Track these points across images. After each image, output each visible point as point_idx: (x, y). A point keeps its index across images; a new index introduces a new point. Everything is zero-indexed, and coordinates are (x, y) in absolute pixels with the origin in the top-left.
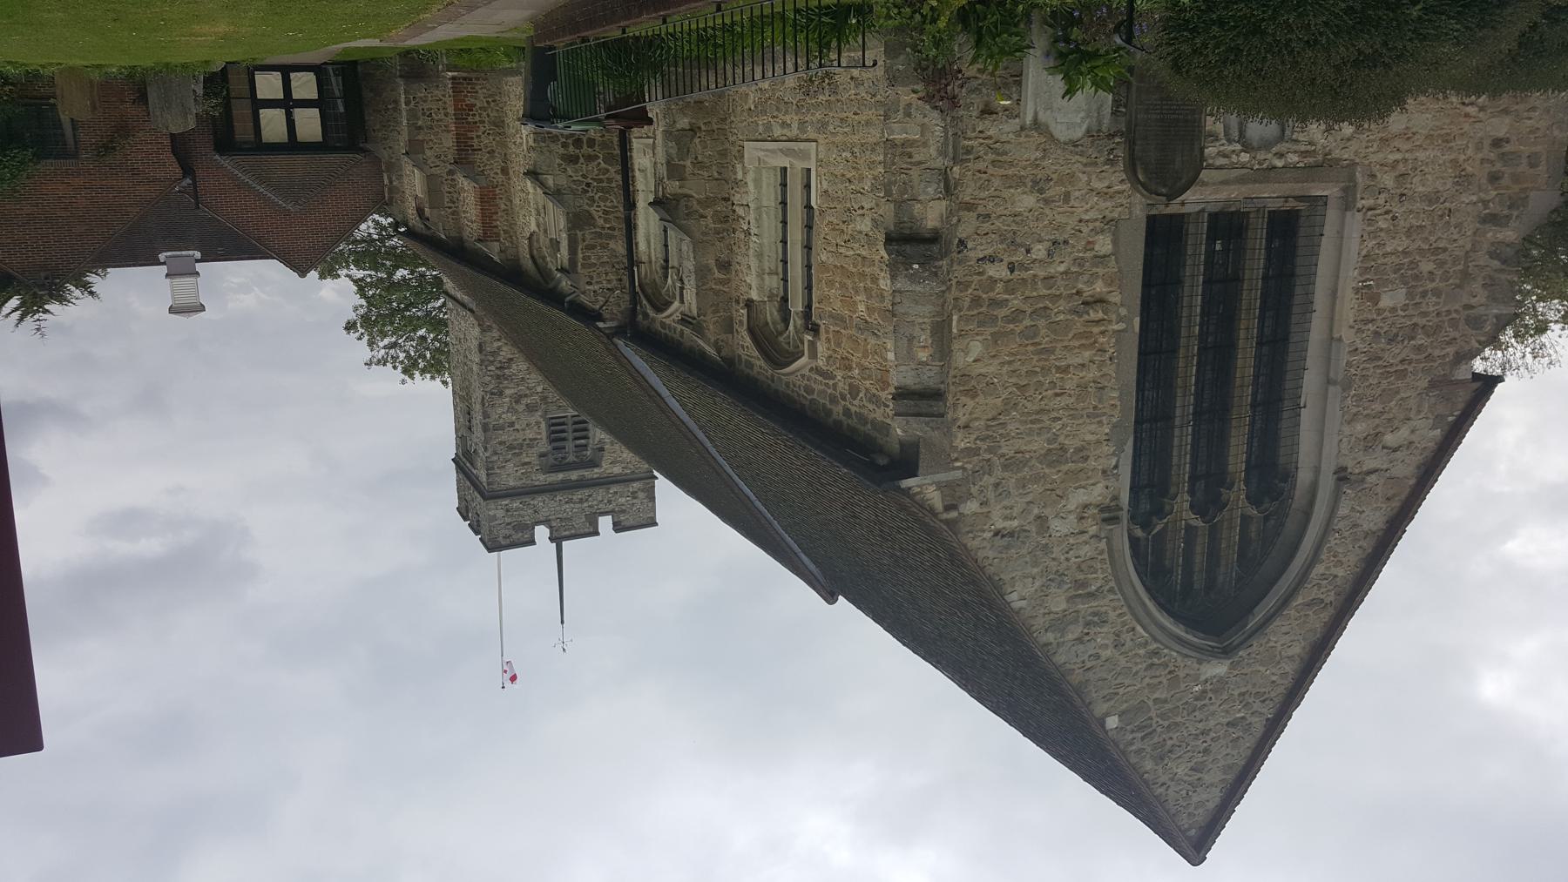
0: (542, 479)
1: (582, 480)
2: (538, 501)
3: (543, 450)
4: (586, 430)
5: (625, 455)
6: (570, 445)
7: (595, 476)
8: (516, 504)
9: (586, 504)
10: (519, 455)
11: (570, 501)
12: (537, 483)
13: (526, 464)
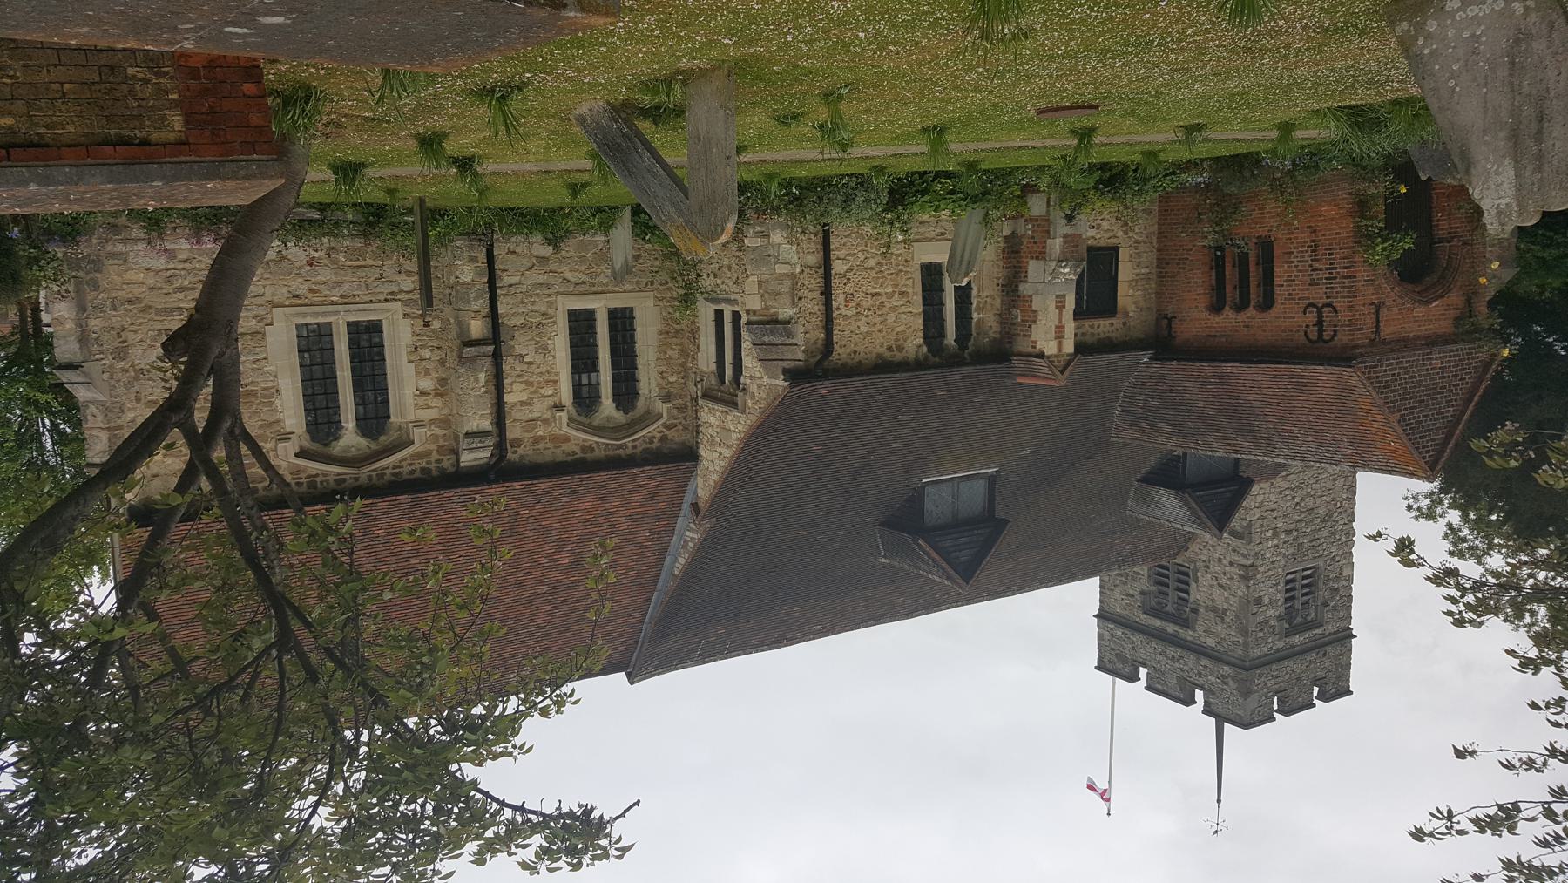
0: (1142, 618)
1: (1175, 636)
2: (1137, 638)
3: (1145, 588)
4: (1188, 584)
5: (1219, 628)
6: (1173, 595)
7: (1189, 638)
8: (1119, 633)
9: (1177, 665)
10: (1125, 583)
11: (1163, 654)
12: (1137, 620)
13: (1129, 595)
